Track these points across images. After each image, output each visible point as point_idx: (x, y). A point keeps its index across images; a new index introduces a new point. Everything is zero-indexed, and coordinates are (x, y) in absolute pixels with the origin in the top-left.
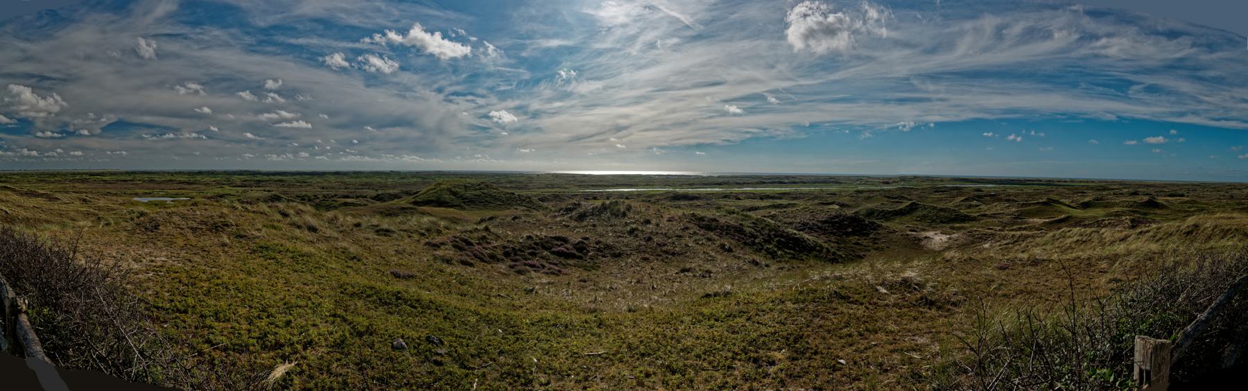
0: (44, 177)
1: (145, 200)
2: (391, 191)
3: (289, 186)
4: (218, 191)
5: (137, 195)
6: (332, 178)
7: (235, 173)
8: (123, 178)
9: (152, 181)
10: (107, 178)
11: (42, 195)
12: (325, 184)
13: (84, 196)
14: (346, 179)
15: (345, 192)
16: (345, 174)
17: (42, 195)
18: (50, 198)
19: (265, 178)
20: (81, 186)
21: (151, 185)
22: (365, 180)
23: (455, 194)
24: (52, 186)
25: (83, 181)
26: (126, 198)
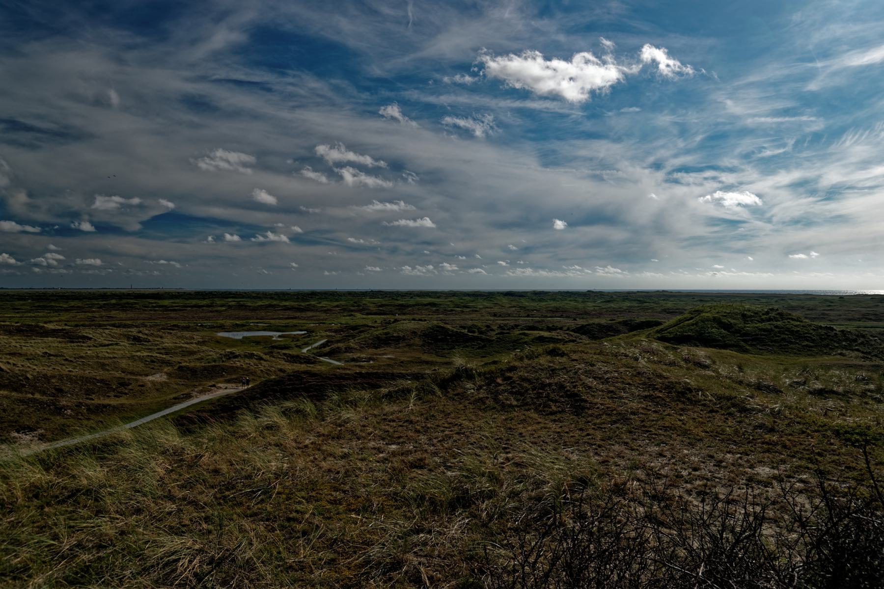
0: (45, 300)
1: (239, 335)
2: (603, 321)
3: (445, 312)
4: (345, 320)
5: (222, 328)
6: (505, 301)
7: (364, 294)
8: (194, 302)
9: (241, 307)
10: (166, 302)
11: (53, 333)
12: (496, 309)
13: (134, 331)
14: (525, 303)
15: (529, 321)
16: (521, 295)
17: (53, 333)
18: (70, 337)
19: (412, 302)
20: (123, 315)
21: (242, 313)
22: (553, 304)
23: (727, 327)
24: (65, 316)
25: (124, 308)
26: (206, 333)
